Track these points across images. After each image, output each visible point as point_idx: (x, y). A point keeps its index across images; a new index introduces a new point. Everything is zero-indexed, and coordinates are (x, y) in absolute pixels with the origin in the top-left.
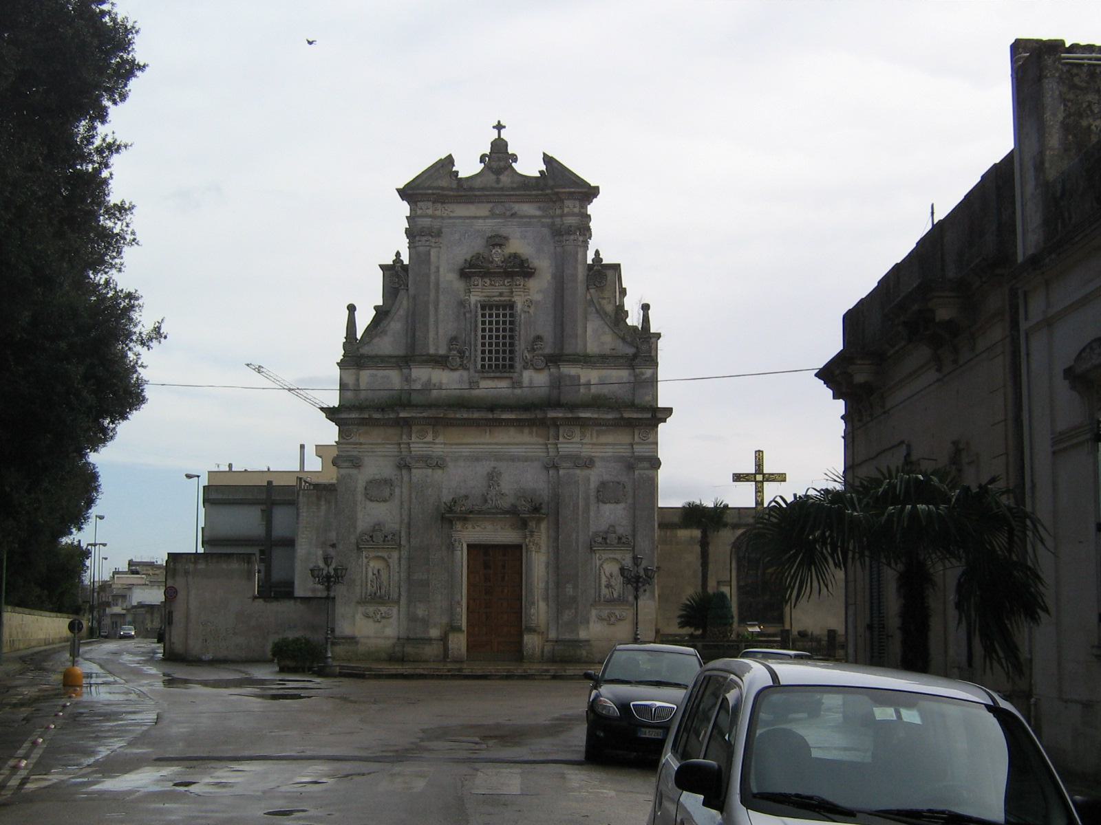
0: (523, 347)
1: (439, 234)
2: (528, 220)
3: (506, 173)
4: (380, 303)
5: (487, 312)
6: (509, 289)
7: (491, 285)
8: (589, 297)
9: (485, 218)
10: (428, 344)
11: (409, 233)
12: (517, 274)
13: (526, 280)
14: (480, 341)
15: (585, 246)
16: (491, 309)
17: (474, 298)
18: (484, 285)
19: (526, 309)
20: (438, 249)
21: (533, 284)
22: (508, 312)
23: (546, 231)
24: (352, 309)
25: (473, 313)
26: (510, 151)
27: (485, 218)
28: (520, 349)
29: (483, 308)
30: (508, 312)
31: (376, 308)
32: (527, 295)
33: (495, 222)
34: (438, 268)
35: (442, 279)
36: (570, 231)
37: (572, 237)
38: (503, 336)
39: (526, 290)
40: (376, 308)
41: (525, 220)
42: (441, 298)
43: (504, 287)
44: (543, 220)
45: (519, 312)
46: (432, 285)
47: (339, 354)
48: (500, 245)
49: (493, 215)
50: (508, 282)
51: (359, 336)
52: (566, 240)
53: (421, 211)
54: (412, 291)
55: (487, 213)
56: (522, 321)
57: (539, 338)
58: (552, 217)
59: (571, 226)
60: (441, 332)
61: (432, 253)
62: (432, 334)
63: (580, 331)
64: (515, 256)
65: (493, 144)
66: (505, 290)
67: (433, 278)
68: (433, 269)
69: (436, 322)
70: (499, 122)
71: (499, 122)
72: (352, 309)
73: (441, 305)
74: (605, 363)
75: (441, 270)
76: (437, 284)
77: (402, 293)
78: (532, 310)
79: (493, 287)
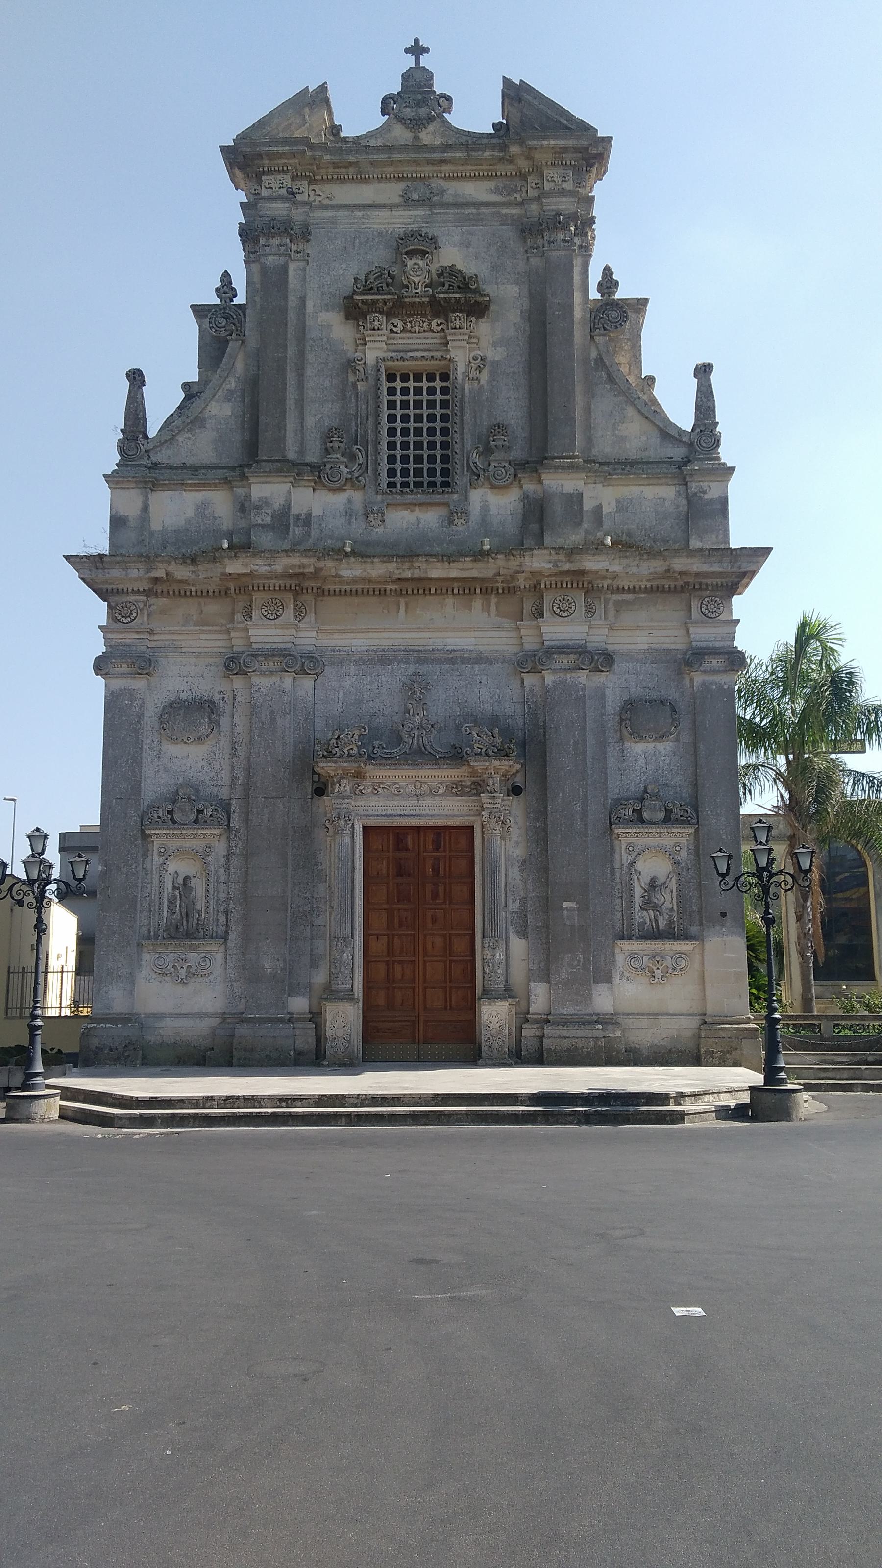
0: (468, 444)
1: (305, 234)
2: (474, 211)
3: (431, 128)
4: (194, 376)
5: (398, 385)
6: (441, 338)
7: (404, 330)
8: (594, 354)
9: (391, 207)
10: (285, 436)
11: (247, 234)
12: (457, 306)
13: (473, 319)
14: (385, 439)
15: (586, 250)
16: (405, 378)
17: (373, 353)
18: (391, 331)
19: (474, 374)
20: (302, 264)
21: (483, 328)
22: (438, 384)
23: (508, 233)
24: (136, 378)
25: (371, 381)
26: (438, 88)
27: (391, 207)
28: (462, 450)
29: (391, 378)
30: (438, 384)
31: (186, 386)
32: (474, 349)
33: (410, 217)
34: (303, 301)
35: (309, 323)
36: (556, 223)
37: (561, 236)
38: (434, 421)
39: (473, 340)
40: (186, 386)
41: (467, 211)
42: (310, 357)
43: (430, 334)
44: (504, 211)
45: (460, 377)
46: (291, 332)
47: (111, 460)
48: (423, 253)
49: (407, 202)
50: (438, 325)
51: (153, 429)
52: (549, 242)
53: (270, 191)
54: (253, 339)
55: (397, 200)
56: (467, 399)
57: (499, 428)
58: (521, 204)
59: (558, 214)
60: (310, 421)
61: (291, 273)
62: (291, 425)
63: (578, 414)
64: (451, 272)
65: (406, 77)
66: (433, 339)
67: (292, 316)
68: (293, 301)
69: (300, 403)
70: (417, 41)
71: (417, 41)
72: (136, 378)
73: (309, 372)
74: (629, 473)
75: (310, 305)
76: (302, 330)
77: (233, 346)
78: (484, 377)
79: (409, 335)
